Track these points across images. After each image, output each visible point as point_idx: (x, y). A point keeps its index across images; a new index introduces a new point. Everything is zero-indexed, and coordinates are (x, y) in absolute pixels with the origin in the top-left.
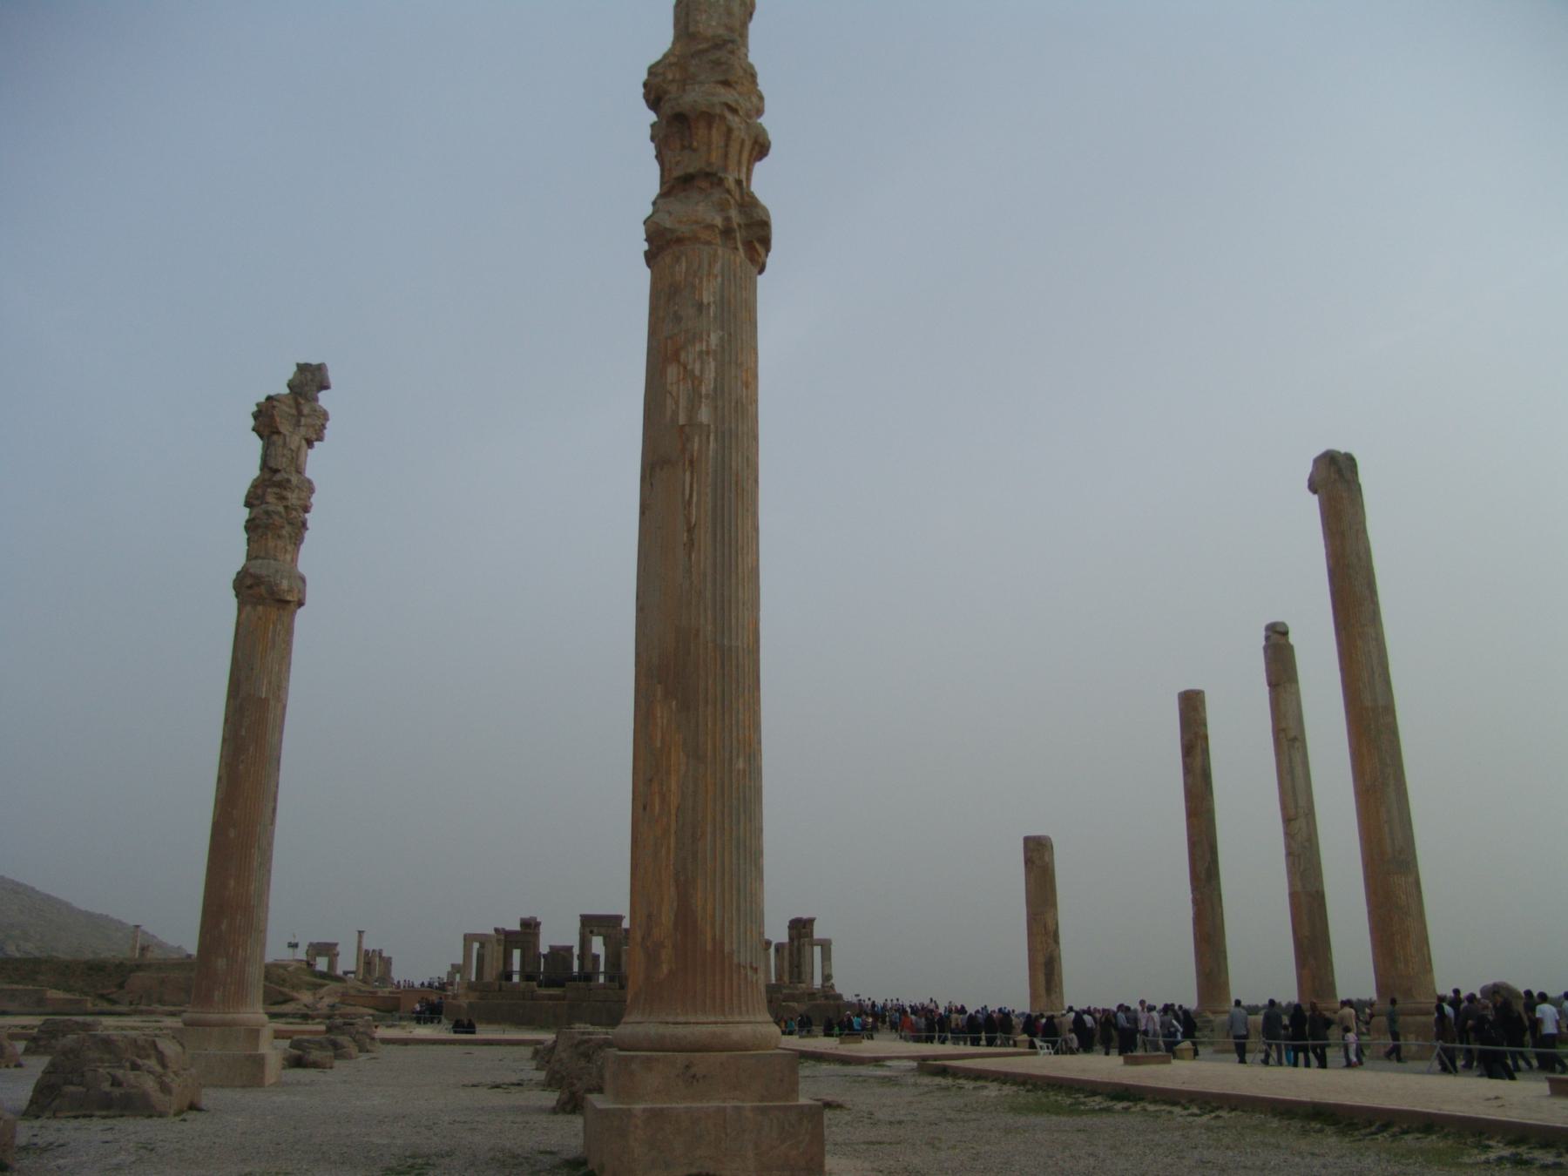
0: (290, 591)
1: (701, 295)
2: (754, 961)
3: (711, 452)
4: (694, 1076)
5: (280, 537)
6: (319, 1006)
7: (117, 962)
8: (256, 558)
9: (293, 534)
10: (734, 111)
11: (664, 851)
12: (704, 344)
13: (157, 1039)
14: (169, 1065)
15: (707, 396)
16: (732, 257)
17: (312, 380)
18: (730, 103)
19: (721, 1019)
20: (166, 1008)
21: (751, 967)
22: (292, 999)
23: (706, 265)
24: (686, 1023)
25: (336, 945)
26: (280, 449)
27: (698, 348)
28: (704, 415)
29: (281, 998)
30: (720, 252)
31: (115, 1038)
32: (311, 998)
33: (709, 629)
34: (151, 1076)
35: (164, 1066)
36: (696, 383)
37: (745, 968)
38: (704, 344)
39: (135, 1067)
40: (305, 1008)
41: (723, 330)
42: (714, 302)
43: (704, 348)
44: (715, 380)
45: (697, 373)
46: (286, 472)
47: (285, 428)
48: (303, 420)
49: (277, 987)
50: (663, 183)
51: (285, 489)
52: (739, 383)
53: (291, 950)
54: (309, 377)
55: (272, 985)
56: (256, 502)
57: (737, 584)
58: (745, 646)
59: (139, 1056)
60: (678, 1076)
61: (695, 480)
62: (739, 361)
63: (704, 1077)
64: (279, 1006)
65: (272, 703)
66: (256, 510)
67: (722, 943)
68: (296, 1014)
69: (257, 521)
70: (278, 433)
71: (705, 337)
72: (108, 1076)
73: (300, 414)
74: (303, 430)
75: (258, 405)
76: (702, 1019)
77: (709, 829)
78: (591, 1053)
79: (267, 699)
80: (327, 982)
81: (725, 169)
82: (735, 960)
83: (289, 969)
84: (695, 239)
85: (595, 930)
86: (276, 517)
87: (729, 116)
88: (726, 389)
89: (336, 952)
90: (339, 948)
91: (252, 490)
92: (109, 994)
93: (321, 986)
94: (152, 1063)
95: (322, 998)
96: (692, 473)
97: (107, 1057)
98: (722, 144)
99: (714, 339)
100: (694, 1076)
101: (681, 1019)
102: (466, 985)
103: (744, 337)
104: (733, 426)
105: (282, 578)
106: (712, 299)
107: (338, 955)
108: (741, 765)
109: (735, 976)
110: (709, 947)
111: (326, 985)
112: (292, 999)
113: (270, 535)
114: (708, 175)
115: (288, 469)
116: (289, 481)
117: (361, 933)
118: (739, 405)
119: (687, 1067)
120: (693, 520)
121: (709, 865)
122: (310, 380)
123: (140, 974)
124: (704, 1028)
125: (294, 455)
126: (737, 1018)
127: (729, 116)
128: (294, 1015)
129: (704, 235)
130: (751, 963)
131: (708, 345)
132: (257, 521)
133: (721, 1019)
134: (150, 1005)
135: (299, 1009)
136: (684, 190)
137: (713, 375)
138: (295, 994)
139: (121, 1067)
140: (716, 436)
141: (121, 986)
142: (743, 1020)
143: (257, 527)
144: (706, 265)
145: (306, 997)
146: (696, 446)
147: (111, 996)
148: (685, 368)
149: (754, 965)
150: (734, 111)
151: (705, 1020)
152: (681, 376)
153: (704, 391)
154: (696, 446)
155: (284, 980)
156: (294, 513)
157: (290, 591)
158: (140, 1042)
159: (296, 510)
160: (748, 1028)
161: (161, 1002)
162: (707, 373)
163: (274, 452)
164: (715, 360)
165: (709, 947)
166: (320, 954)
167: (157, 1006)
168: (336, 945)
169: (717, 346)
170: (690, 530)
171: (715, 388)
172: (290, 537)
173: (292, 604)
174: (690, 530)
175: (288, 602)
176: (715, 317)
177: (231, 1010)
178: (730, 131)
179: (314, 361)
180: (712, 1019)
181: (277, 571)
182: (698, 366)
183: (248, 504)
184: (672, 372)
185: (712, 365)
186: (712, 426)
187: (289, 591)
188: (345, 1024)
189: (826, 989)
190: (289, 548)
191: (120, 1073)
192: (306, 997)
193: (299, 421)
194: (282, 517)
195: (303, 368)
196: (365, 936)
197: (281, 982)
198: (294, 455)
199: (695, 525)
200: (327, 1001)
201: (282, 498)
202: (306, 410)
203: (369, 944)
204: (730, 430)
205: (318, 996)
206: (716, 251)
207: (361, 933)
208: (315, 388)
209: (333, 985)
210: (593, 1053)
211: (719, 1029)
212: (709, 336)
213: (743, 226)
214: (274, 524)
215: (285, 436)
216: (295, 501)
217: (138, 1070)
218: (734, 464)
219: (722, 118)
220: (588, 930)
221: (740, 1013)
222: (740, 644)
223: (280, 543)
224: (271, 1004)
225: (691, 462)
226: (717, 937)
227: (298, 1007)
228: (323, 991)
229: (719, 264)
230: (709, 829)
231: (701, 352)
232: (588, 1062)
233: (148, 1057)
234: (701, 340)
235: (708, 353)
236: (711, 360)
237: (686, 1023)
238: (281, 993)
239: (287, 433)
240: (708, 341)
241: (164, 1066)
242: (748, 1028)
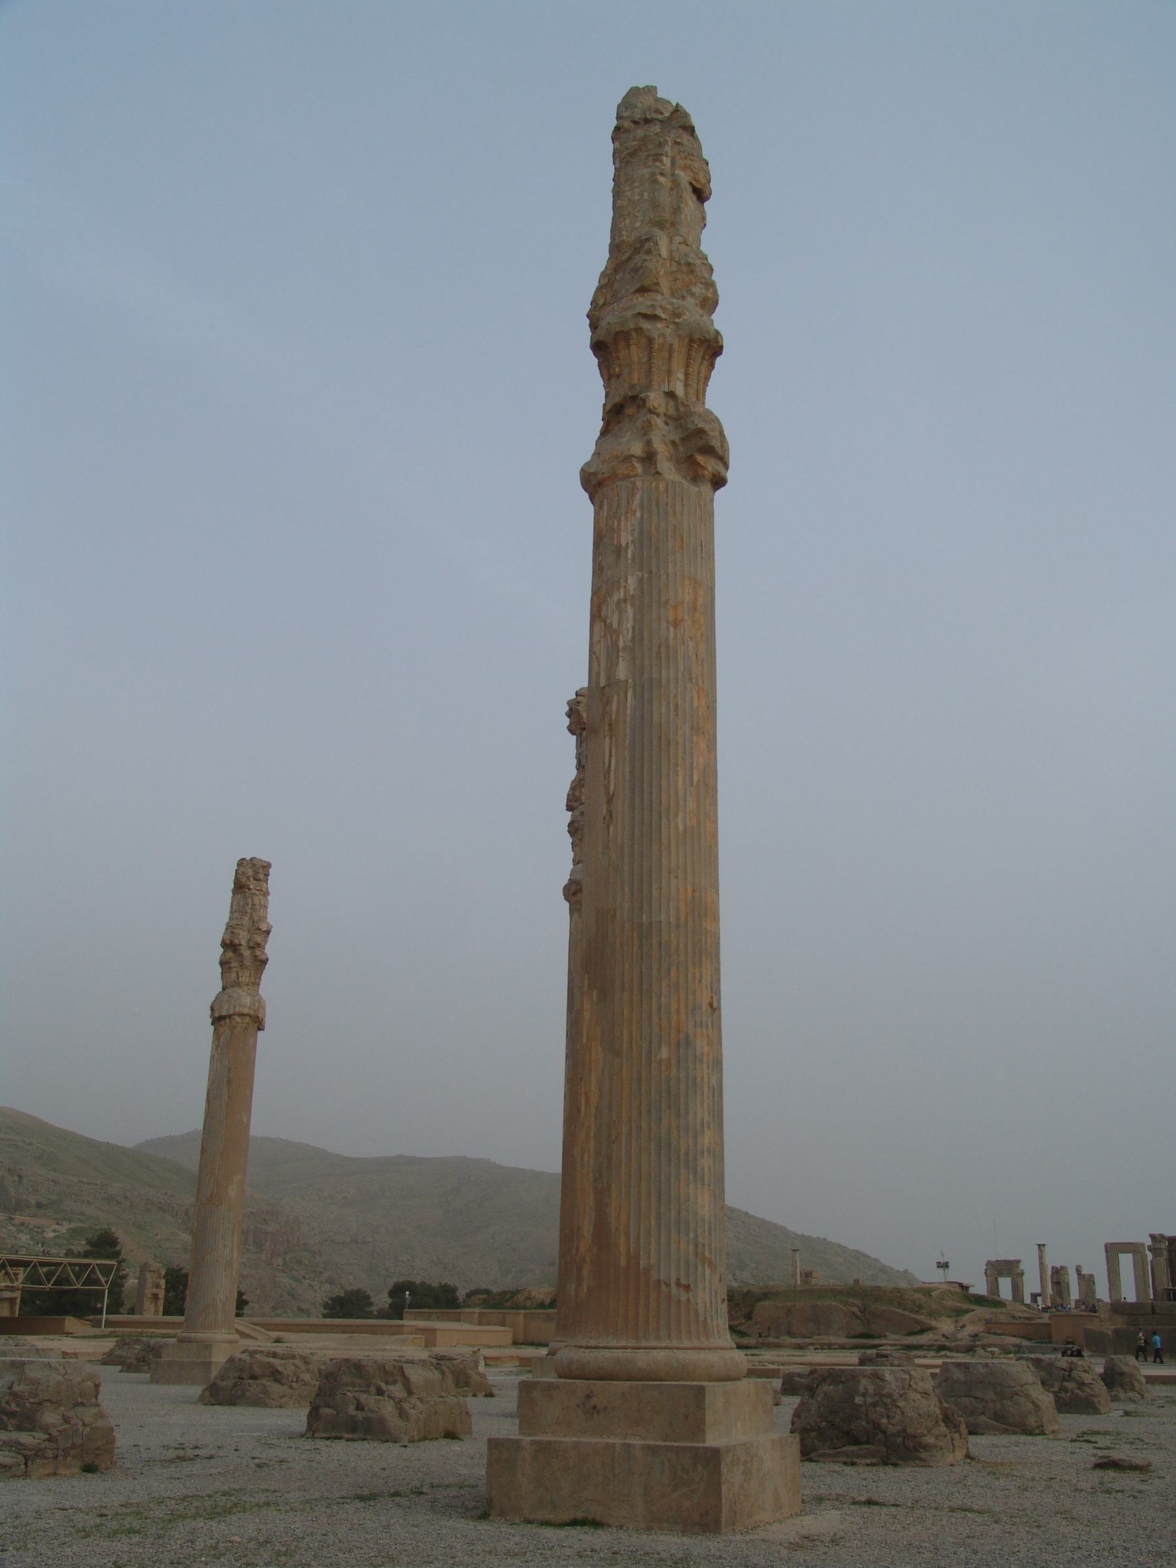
1: (619, 537)
2: (682, 1273)
3: (628, 710)
4: (594, 1408)
6: (959, 1336)
7: (745, 1290)
8: (578, 863)
10: (654, 318)
11: (586, 1155)
12: (622, 591)
13: (404, 1365)
14: (415, 1391)
15: (625, 648)
16: (654, 484)
18: (643, 311)
19: (633, 1343)
20: (794, 1341)
21: (678, 1284)
22: (931, 1329)
23: (624, 503)
24: (595, 1348)
25: (1018, 1262)
27: (615, 598)
28: (622, 672)
29: (918, 1328)
30: (639, 484)
31: (365, 1363)
32: (952, 1327)
33: (626, 905)
34: (392, 1401)
35: (410, 1393)
36: (614, 636)
37: (668, 1285)
38: (622, 591)
39: (380, 1392)
40: (944, 1339)
41: (641, 569)
42: (633, 542)
43: (622, 596)
44: (634, 628)
45: (615, 625)
49: (912, 1315)
52: (664, 624)
53: (941, 1271)
55: (907, 1313)
56: (575, 805)
57: (660, 851)
58: (672, 919)
59: (387, 1383)
60: (578, 1406)
61: (613, 745)
62: (663, 600)
63: (605, 1408)
64: (915, 1337)
66: (577, 812)
67: (638, 1256)
68: (932, 1345)
69: (576, 825)
71: (623, 583)
72: (354, 1400)
76: (686, 1343)
77: (625, 1129)
78: (815, 1386)
80: (974, 1307)
82: (654, 1275)
83: (933, 1293)
84: (614, 477)
88: (646, 636)
89: (1019, 1271)
90: (1022, 1266)
91: (571, 792)
92: (736, 1326)
93: (967, 1311)
94: (397, 1390)
95: (964, 1326)
96: (611, 738)
97: (358, 1381)
98: (645, 359)
99: (632, 582)
100: (594, 1408)
101: (593, 1343)
103: (671, 571)
104: (655, 675)
106: (630, 538)
107: (1022, 1274)
108: (664, 1053)
109: (653, 1295)
110: (623, 1263)
111: (974, 1310)
112: (931, 1329)
114: (634, 398)
117: (1041, 1246)
118: (663, 650)
119: (588, 1397)
120: (612, 789)
121: (623, 1170)
123: (766, 1303)
124: (608, 1354)
126: (653, 1343)
127: (646, 325)
128: (929, 1347)
129: (622, 470)
130: (678, 1279)
131: (625, 592)
132: (576, 825)
133: (633, 1343)
134: (778, 1338)
135: (936, 1340)
136: (619, 422)
137: (631, 623)
138: (933, 1323)
139: (368, 1392)
140: (634, 690)
141: (749, 1317)
142: (660, 1345)
143: (577, 830)
144: (624, 503)
145: (946, 1326)
146: (614, 708)
147: (739, 1328)
148: (605, 622)
149: (683, 1281)
150: (654, 318)
151: (614, 1344)
152: (603, 633)
153: (621, 644)
154: (614, 708)
155: (920, 1306)
158: (387, 1368)
160: (660, 1355)
161: (790, 1333)
162: (625, 623)
164: (633, 605)
165: (623, 1263)
166: (1001, 1274)
167: (785, 1338)
168: (1018, 1262)
169: (635, 590)
170: (609, 801)
171: (633, 637)
174: (609, 801)
176: (633, 558)
177: (216, 1331)
178: (650, 341)
180: (622, 1343)
182: (616, 618)
183: (569, 808)
185: (630, 611)
186: (630, 681)
188: (878, 1356)
191: (363, 1397)
192: (946, 1326)
196: (1047, 1250)
197: (917, 1309)
199: (613, 795)
200: (970, 1329)
203: (1052, 1261)
204: (651, 678)
205: (961, 1324)
206: (634, 483)
207: (1041, 1246)
209: (980, 1311)
210: (817, 1385)
211: (628, 1354)
212: (627, 582)
213: (678, 442)
217: (382, 1395)
218: (656, 716)
219: (639, 330)
221: (658, 1337)
222: (663, 917)
224: (906, 1335)
225: (610, 725)
226: (631, 1251)
227: (936, 1337)
228: (966, 1318)
229: (638, 496)
230: (625, 1129)
231: (618, 603)
232: (812, 1397)
233: (395, 1382)
234: (619, 588)
235: (625, 600)
236: (629, 607)
237: (595, 1348)
238: (917, 1321)
240: (625, 587)
241: (410, 1393)
242: (660, 1355)
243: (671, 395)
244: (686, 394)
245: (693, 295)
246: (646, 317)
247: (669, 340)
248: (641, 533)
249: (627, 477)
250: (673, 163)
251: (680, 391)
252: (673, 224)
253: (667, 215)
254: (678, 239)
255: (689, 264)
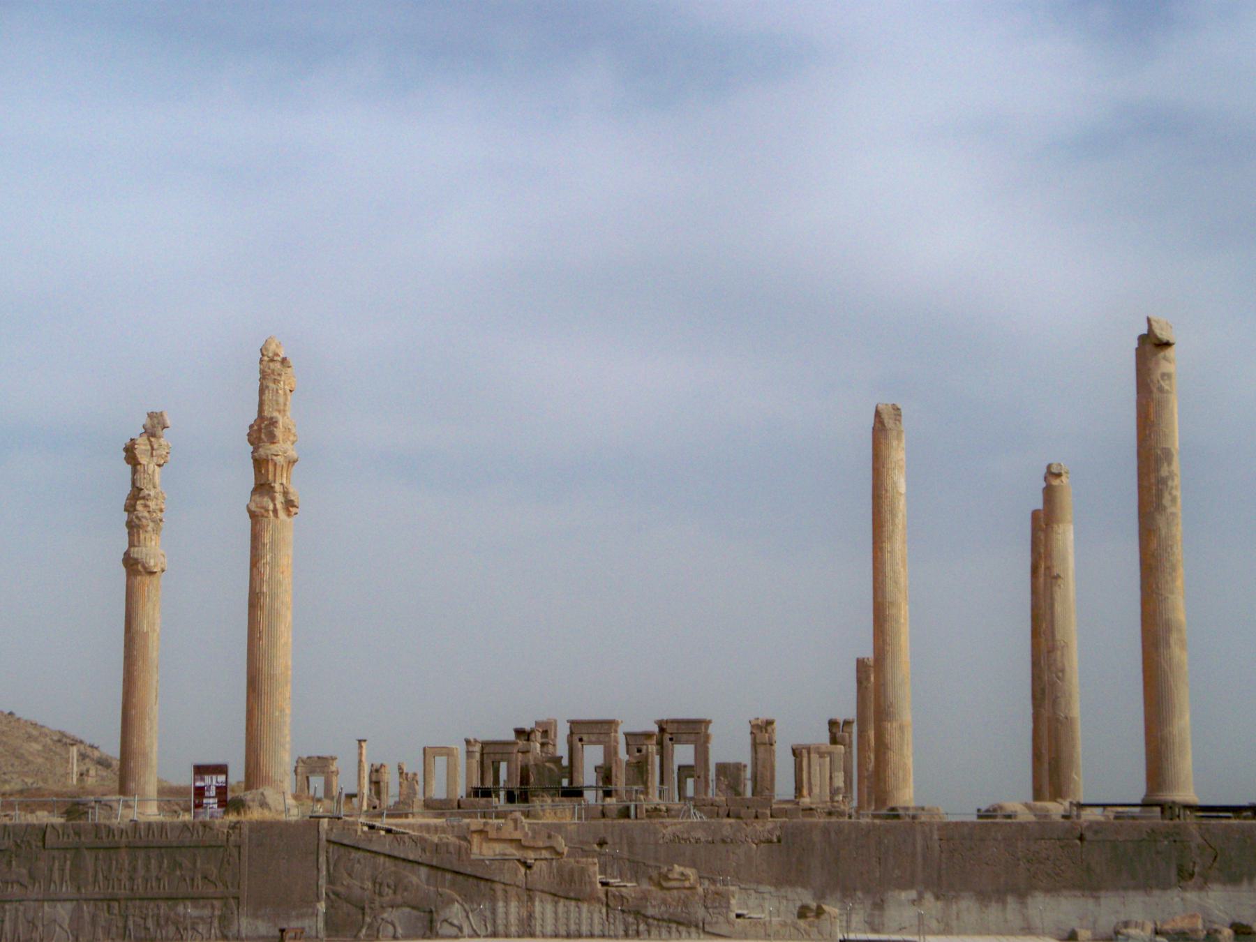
0: (155, 566)
5: (146, 531)
9: (155, 528)
17: (158, 423)
26: (142, 474)
46: (147, 489)
47: (143, 460)
48: (154, 453)
50: (255, 484)
51: (147, 500)
54: (156, 421)
65: (150, 634)
70: (140, 464)
73: (152, 449)
74: (155, 459)
75: (125, 444)
79: (148, 632)
81: (275, 481)
85: (585, 738)
86: (144, 520)
87: (275, 458)
102: (422, 803)
105: (150, 559)
113: (141, 532)
115: (148, 487)
116: (149, 495)
122: (154, 427)
125: (151, 477)
127: (275, 458)
150: (277, 455)
156: (155, 514)
157: (155, 566)
159: (155, 512)
163: (138, 477)
166: (313, 772)
172: (153, 531)
173: (158, 573)
175: (156, 572)
179: (157, 410)
181: (147, 555)
184: (255, 569)
187: (154, 566)
189: (836, 804)
190: (153, 538)
193: (152, 454)
194: (147, 519)
195: (151, 415)
198: (151, 477)
201: (146, 506)
202: (156, 446)
208: (160, 429)
214: (142, 525)
215: (144, 465)
216: (154, 507)
219: (272, 460)
220: (576, 738)
223: (148, 536)
239: (145, 463)
243: (282, 484)
244: (287, 482)
245: (290, 440)
246: (275, 455)
247: (282, 463)
248: (272, 539)
249: (267, 517)
250: (284, 383)
251: (284, 481)
252: (284, 411)
253: (282, 408)
254: (286, 417)
255: (289, 429)
